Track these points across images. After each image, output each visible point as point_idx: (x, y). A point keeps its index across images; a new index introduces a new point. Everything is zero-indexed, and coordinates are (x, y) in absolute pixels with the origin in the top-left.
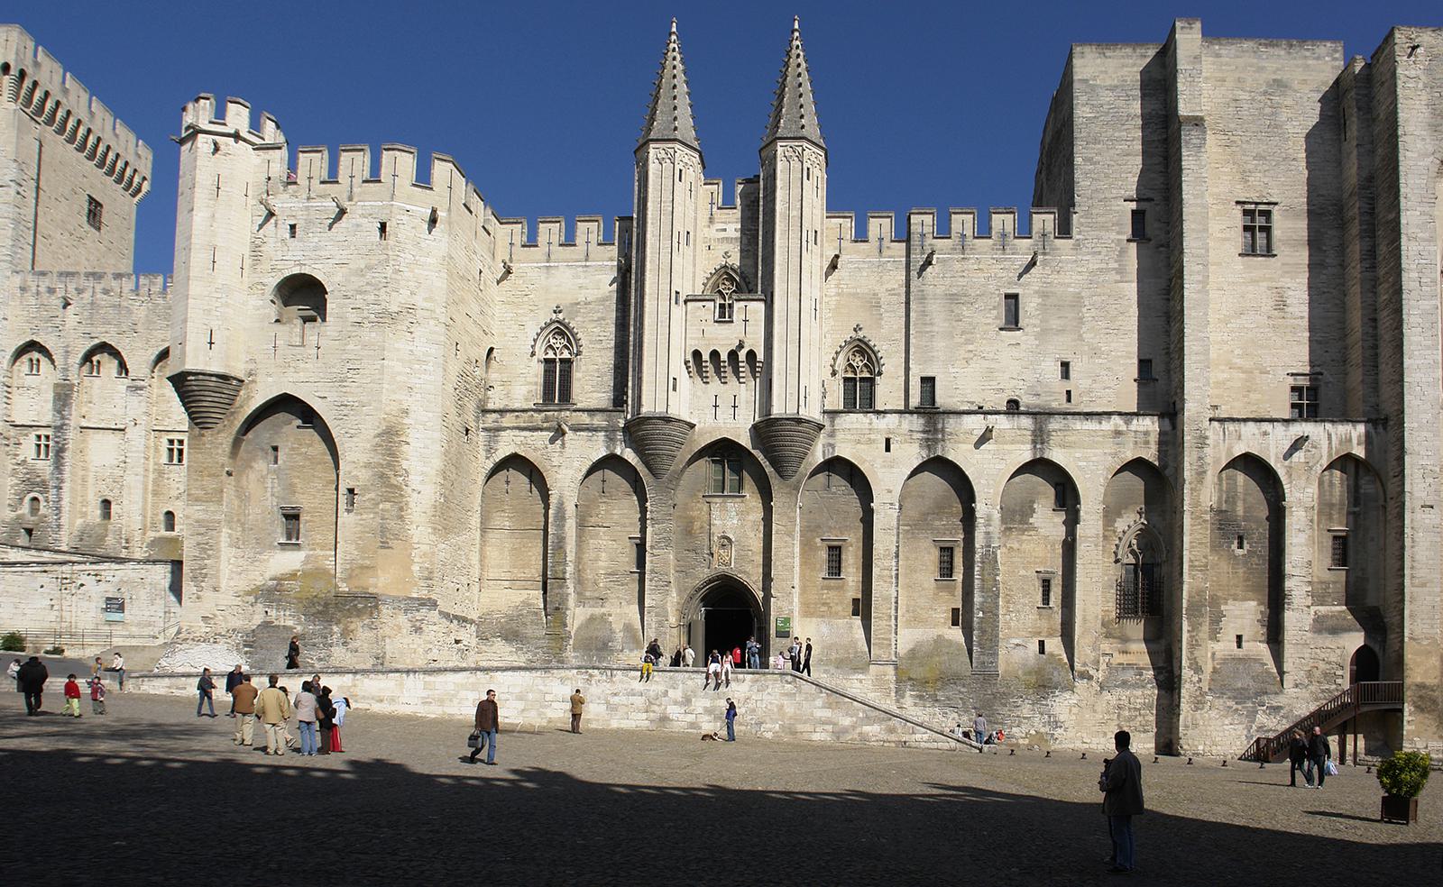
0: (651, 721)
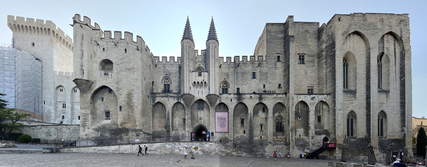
0: (189, 153)
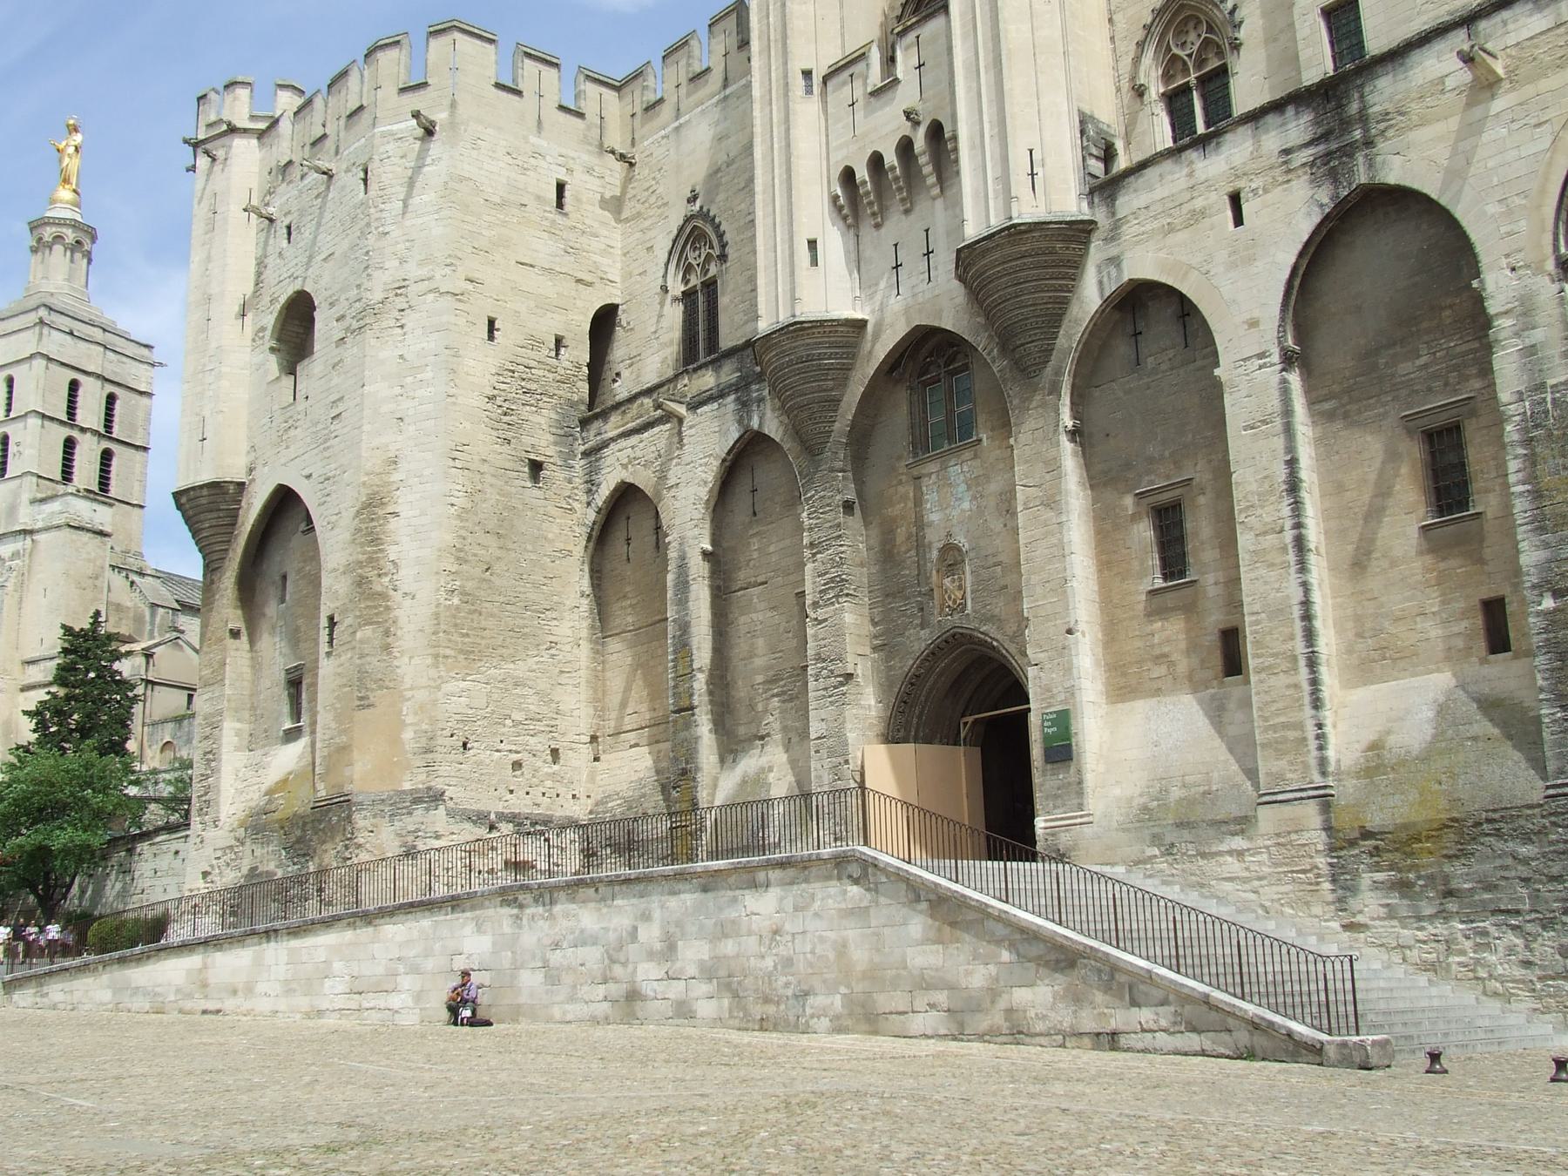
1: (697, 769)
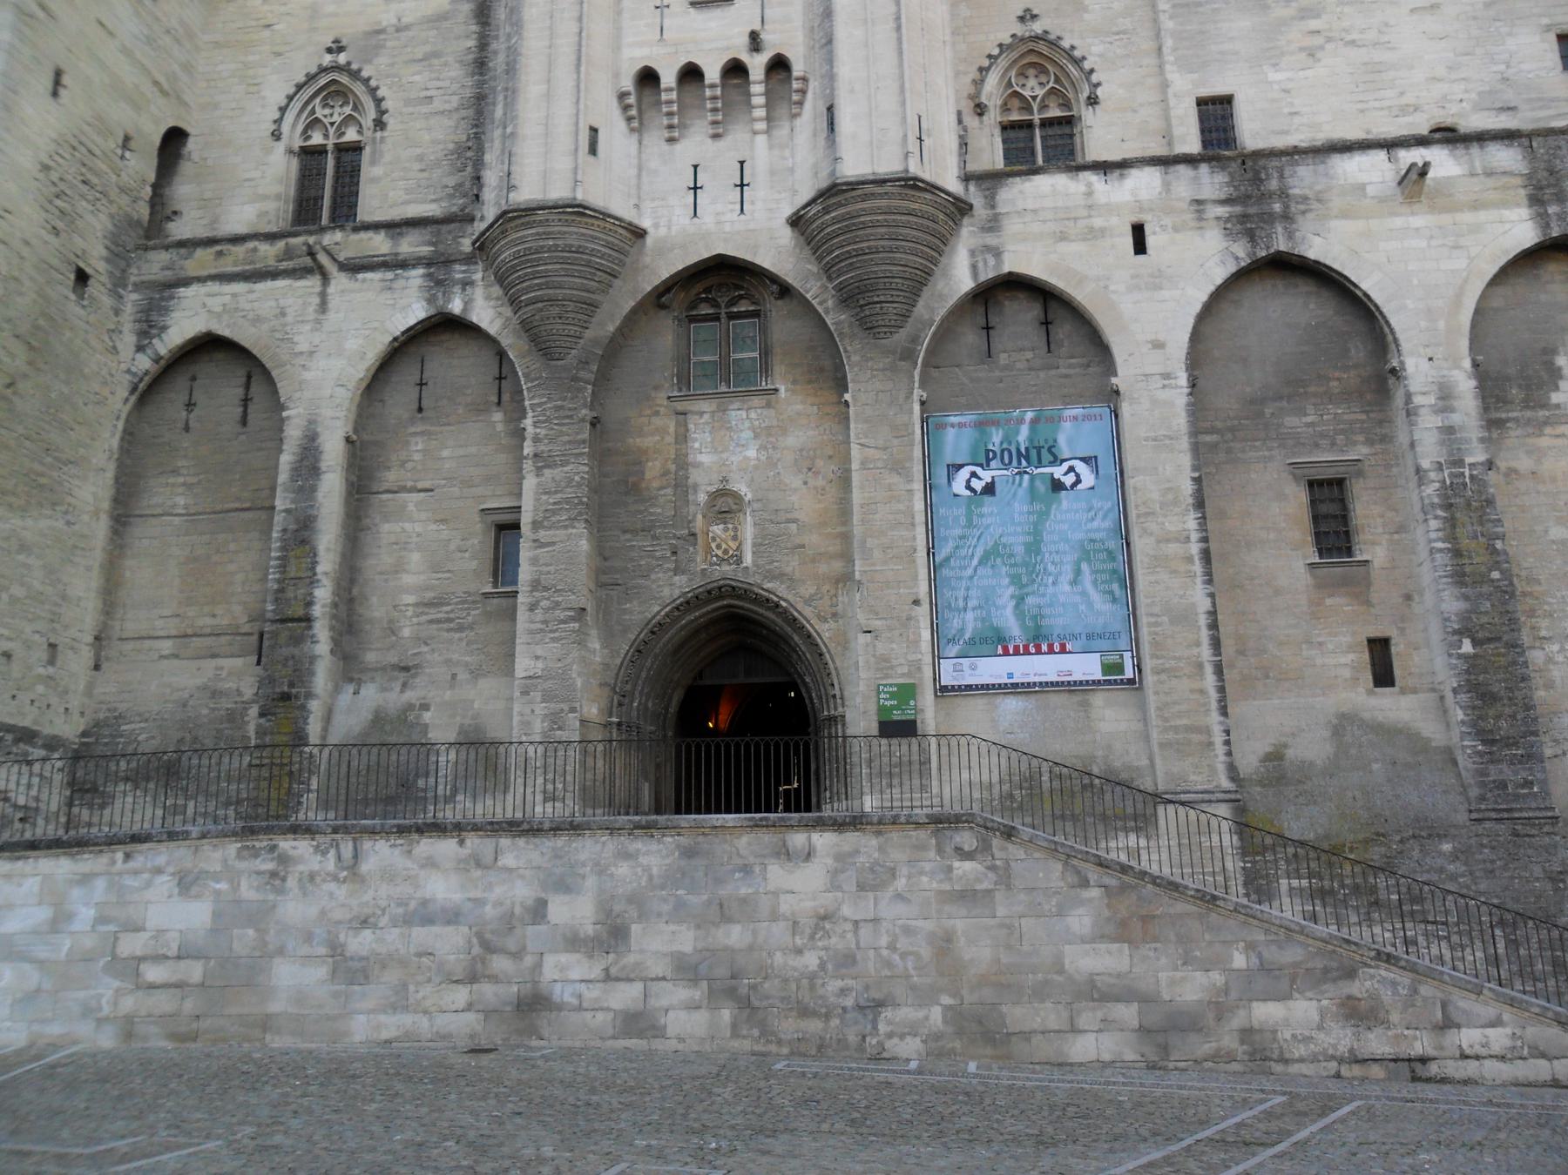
0: (488, 1013)
1: (309, 695)
